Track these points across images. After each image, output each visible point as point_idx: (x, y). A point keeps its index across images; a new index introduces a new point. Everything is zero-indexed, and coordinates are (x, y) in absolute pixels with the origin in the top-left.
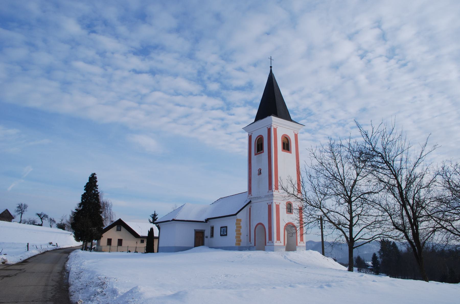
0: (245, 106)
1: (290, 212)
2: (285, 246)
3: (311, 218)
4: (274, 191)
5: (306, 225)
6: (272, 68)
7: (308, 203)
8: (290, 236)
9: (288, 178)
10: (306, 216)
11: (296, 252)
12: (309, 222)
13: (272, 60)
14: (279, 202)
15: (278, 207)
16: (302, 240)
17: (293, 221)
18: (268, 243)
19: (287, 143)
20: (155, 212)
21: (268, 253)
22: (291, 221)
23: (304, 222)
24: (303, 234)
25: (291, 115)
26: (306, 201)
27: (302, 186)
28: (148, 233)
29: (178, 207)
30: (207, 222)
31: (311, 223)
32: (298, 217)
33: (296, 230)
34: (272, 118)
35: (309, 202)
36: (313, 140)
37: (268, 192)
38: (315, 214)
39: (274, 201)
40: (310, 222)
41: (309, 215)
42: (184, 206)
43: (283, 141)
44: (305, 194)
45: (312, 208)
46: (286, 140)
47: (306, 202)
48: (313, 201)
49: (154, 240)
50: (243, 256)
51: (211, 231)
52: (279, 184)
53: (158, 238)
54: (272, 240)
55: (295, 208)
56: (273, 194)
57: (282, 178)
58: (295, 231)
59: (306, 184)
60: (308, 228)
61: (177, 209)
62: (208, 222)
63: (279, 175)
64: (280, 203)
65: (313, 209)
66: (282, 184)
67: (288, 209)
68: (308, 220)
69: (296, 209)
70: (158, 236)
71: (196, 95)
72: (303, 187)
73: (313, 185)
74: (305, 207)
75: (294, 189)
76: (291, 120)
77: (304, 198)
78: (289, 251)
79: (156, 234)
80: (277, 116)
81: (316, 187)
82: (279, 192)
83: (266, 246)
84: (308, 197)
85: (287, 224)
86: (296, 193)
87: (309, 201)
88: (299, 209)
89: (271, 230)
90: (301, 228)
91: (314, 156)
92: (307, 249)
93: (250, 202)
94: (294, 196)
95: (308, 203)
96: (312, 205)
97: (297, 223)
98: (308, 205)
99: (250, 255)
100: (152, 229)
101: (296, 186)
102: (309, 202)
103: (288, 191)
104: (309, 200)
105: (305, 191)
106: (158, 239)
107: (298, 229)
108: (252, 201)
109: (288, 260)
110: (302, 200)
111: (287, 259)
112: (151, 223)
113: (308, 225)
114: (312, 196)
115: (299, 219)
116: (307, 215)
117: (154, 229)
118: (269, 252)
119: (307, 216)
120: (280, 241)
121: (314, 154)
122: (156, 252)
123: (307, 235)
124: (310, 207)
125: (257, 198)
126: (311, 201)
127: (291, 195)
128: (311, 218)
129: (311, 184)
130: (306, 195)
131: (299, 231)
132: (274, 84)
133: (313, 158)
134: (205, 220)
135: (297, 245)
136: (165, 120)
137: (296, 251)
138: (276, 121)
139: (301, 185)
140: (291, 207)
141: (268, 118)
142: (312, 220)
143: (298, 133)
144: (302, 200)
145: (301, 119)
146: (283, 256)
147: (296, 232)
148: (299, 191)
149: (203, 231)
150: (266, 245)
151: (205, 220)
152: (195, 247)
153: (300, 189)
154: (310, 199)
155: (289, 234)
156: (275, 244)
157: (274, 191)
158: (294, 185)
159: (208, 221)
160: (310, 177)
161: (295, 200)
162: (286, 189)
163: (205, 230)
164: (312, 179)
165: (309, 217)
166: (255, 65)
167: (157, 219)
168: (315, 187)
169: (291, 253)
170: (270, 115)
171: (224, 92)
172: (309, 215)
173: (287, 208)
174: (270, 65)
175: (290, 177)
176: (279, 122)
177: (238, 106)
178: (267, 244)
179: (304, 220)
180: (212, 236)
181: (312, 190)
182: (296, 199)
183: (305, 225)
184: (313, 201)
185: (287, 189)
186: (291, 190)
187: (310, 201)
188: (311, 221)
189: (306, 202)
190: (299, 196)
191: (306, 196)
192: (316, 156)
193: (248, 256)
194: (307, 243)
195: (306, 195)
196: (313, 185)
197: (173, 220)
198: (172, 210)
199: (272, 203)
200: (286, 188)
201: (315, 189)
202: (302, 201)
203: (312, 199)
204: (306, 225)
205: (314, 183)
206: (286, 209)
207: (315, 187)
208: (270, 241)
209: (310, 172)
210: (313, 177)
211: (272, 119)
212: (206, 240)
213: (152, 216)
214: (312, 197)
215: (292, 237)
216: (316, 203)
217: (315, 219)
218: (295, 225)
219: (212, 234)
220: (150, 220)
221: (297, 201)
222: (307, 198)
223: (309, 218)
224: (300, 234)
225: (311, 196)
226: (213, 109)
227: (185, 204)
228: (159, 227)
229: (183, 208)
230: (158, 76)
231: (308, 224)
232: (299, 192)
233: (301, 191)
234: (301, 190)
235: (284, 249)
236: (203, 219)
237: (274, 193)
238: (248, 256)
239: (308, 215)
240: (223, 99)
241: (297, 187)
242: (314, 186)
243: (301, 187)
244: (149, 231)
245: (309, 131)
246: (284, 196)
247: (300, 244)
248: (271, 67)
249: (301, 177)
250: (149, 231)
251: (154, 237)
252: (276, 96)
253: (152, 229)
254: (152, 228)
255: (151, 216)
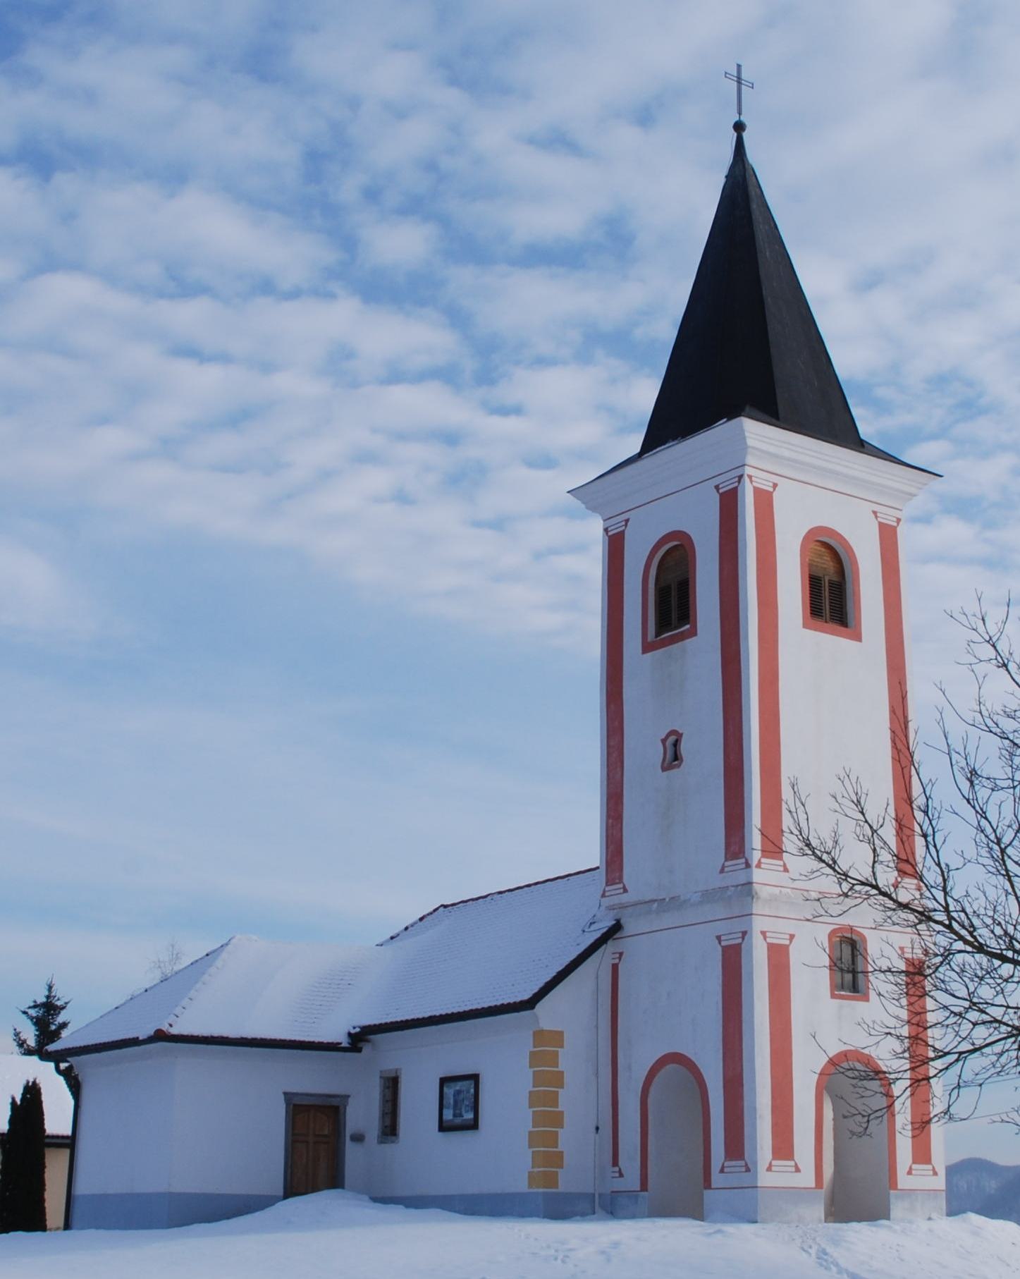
0: (583, 357)
1: (855, 988)
2: (823, 1193)
3: (975, 1024)
4: (758, 866)
5: (947, 1068)
6: (745, 135)
7: (961, 938)
8: (853, 1133)
9: (838, 788)
10: (947, 1014)
11: (890, 1227)
12: (966, 1046)
13: (743, 87)
14: (789, 927)
15: (779, 957)
16: (922, 1154)
17: (873, 1040)
18: (722, 1171)
19: (835, 578)
20: (50, 988)
21: (719, 1231)
22: (859, 1041)
23: (935, 1050)
24: (929, 1122)
25: (855, 412)
26: (944, 925)
27: (925, 836)
28: (7, 1113)
29: (186, 962)
30: (359, 1050)
31: (978, 1053)
32: (897, 1018)
33: (888, 1095)
34: (743, 431)
35: (963, 927)
36: (988, 563)
37: (722, 871)
38: (1000, 1000)
39: (758, 924)
40: (972, 1047)
41: (967, 1004)
42: (224, 955)
43: (810, 566)
44: (940, 880)
45: (980, 964)
46: (828, 564)
47: (949, 927)
48: (989, 921)
49: (43, 1158)
50: (571, 1250)
51: (384, 1101)
52: (787, 822)
53: (69, 1143)
54: (744, 1159)
55: (885, 968)
56: (750, 883)
57: (803, 789)
58: (884, 1102)
59: (946, 824)
60: (959, 1086)
61: (180, 971)
62: (367, 1049)
63: (787, 771)
64: (792, 937)
65: (988, 973)
66: (803, 824)
67: (842, 970)
68: (959, 1039)
69: (889, 970)
70: (68, 1131)
71: (295, 294)
72: (930, 839)
73: (989, 830)
74: (939, 959)
75: (874, 850)
76: (860, 445)
77: (937, 906)
78: (847, 1220)
79: (57, 1119)
80: (778, 418)
81: (1006, 840)
82: (786, 870)
83: (707, 1193)
84: (957, 901)
85: (833, 1062)
86: (886, 877)
87: (966, 923)
88: (907, 973)
89: (741, 1097)
90: (920, 1082)
91: (993, 654)
92: (954, 1210)
93: (616, 928)
94: (875, 892)
95: (961, 938)
96: (981, 949)
97: (897, 1056)
98: (959, 945)
99: (616, 1245)
100: (32, 1092)
101: (889, 833)
102: (963, 932)
103: (843, 865)
104: (962, 915)
105: (939, 865)
106: (67, 1152)
107: (897, 1089)
108: (630, 927)
109: (840, 1271)
110: (925, 916)
111: (834, 1269)
112: (29, 1052)
113: (961, 1063)
114: (984, 893)
115: (905, 1031)
116: (956, 1010)
117: (43, 1091)
118: (730, 1228)
119: (956, 1014)
120: (792, 1163)
121: (994, 646)
122: (58, 1229)
123: (952, 1125)
124: (968, 957)
125: (655, 905)
126: (976, 922)
127: (858, 888)
128: (975, 1024)
129: (976, 824)
130: (944, 889)
131: (908, 1103)
132: (760, 230)
133: (991, 668)
134: (350, 1034)
135: (893, 1183)
136: (113, 439)
137: (888, 1218)
138: (772, 449)
139: (917, 828)
140: (860, 958)
141: (722, 430)
142: (981, 1034)
143: (899, 520)
144: (925, 916)
145: (915, 436)
146: (813, 1251)
147: (891, 1106)
148: (906, 864)
149: (335, 1102)
150: (707, 1184)
151: (350, 1034)
152: (291, 1200)
153: (913, 854)
154: (969, 910)
155: (845, 1117)
156: (765, 1179)
157: (755, 862)
158: (874, 831)
159: (368, 1041)
160: (972, 782)
161: (879, 916)
162: (829, 853)
163: (349, 1096)
164: (982, 793)
165: (967, 1016)
166: (645, 117)
167: (64, 1033)
168: (999, 842)
169: (859, 1234)
170: (733, 412)
171: (462, 277)
172: (967, 1004)
173: (835, 965)
174: (737, 119)
175: (854, 781)
176: (787, 453)
177: (542, 362)
178: (717, 1179)
179: (938, 1038)
180: (390, 1130)
181: (980, 860)
182: (889, 913)
183: (939, 1064)
184: (987, 926)
185: (835, 854)
186: (856, 859)
187: (972, 925)
188: (979, 1043)
189: (949, 927)
190: (903, 897)
191: (946, 893)
192: (1005, 654)
193: (603, 1252)
194: (951, 1171)
195: (944, 889)
196: (989, 830)
197: (160, 1036)
198: (152, 978)
199: (744, 933)
200: (830, 844)
201: (1003, 851)
202: (921, 922)
203: (982, 911)
204: (947, 1068)
205: (992, 814)
206: (827, 971)
207: (998, 843)
208: (734, 1163)
209: (971, 749)
210: (986, 783)
211: (747, 434)
212: (353, 1156)
213: (33, 1012)
214: (982, 900)
215: (865, 1138)
216: (1006, 933)
217: (1003, 1028)
218: (885, 1069)
219: (388, 1122)
220: (23, 1036)
221: (894, 924)
222: (951, 908)
223: (966, 1026)
224: (909, 1119)
225: (975, 893)
226: (395, 375)
227: (227, 944)
228: (76, 1078)
229: (219, 963)
230: (66, 183)
231: (957, 1060)
232: (905, 873)
233: (920, 866)
234: (919, 859)
235: (819, 1210)
236: (335, 1032)
237: (758, 876)
238: (603, 1252)
239: (959, 1005)
240: (457, 318)
241: (892, 842)
242: (992, 837)
243: (919, 842)
244: (19, 1102)
245: (964, 508)
246: (814, 895)
247: (910, 1176)
248: (739, 127)
249: (915, 779)
250: (13, 1099)
251: (48, 1137)
252: (769, 301)
253: (32, 1092)
254: (34, 1083)
255: (25, 1013)
